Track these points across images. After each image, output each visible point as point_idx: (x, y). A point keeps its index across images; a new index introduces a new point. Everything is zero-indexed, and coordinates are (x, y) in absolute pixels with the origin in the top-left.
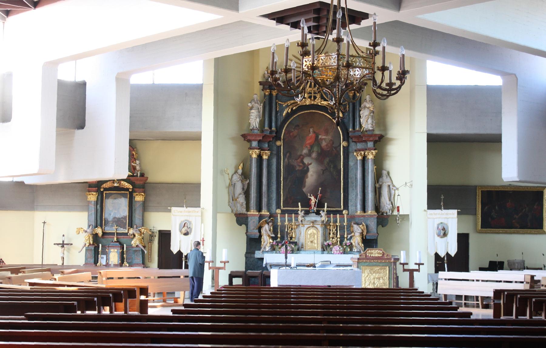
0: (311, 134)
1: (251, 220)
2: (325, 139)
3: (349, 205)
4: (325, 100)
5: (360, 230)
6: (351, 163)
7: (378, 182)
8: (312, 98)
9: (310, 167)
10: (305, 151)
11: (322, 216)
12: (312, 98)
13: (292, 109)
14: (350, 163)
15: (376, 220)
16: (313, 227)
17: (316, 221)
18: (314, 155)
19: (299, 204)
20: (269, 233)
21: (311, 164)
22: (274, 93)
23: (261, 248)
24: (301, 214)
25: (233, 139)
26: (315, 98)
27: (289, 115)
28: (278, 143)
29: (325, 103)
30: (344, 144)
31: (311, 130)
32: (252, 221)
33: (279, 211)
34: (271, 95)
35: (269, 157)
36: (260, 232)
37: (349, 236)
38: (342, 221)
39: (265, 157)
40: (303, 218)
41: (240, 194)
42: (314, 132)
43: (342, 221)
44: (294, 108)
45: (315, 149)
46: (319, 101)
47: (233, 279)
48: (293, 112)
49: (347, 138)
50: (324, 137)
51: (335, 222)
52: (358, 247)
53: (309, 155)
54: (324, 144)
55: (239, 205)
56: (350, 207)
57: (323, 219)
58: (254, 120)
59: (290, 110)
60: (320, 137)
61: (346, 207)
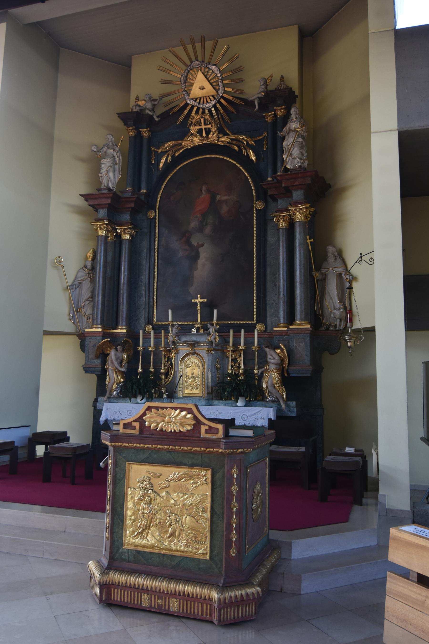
0: (204, 195)
1: (90, 342)
2: (226, 201)
3: (268, 314)
4: (225, 134)
5: (277, 358)
6: (271, 239)
7: (318, 269)
8: (204, 134)
9: (201, 250)
10: (194, 224)
11: (209, 334)
12: (204, 134)
13: (173, 157)
14: (269, 239)
15: (308, 339)
16: (193, 353)
17: (198, 342)
18: (208, 230)
19: (170, 311)
20: (116, 364)
21: (202, 245)
22: (145, 133)
23: (106, 391)
24: (173, 331)
25: (80, 212)
26: (208, 131)
27: (169, 167)
28: (151, 214)
29: (225, 139)
30: (259, 205)
31: (204, 188)
32: (92, 344)
33: (149, 328)
34: (138, 136)
35: (132, 237)
36: (104, 363)
37: (260, 371)
38: (249, 343)
39: (126, 237)
40: (177, 338)
41: (87, 300)
42: (208, 191)
43: (249, 343)
44: (177, 154)
45: (210, 219)
46: (213, 138)
47: (44, 446)
48: (176, 161)
49: (263, 195)
50: (224, 198)
51: (236, 344)
52: (273, 391)
53: (201, 230)
54: (225, 209)
55: (85, 319)
56: (268, 319)
57: (210, 338)
58: (111, 176)
59: (170, 158)
60: (218, 197)
61: (262, 318)
